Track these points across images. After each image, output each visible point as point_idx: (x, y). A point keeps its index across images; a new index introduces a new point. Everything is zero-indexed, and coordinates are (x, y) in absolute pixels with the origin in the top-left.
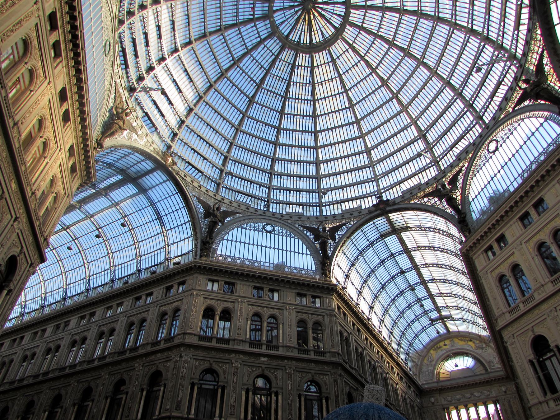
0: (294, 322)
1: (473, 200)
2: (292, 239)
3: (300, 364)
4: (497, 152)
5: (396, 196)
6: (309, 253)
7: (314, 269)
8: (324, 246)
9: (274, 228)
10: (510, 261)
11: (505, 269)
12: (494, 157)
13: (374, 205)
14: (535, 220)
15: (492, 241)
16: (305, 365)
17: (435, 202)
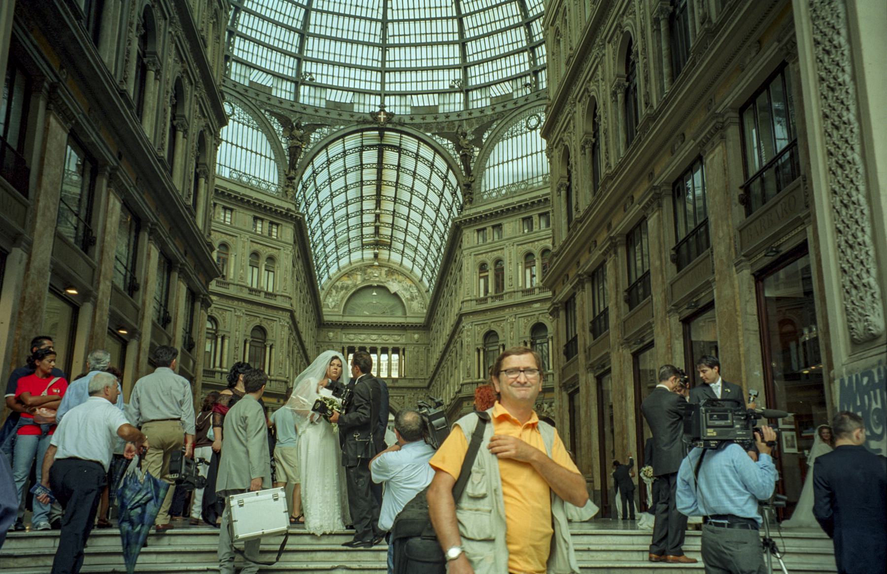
0: (247, 254)
1: (489, 167)
2: (255, 131)
3: (250, 307)
4: (534, 132)
6: (273, 157)
7: (276, 182)
8: (294, 151)
9: (233, 109)
10: (496, 254)
11: (489, 259)
12: (529, 134)
13: (372, 114)
14: (534, 230)
15: (489, 225)
16: (255, 308)
17: (448, 144)
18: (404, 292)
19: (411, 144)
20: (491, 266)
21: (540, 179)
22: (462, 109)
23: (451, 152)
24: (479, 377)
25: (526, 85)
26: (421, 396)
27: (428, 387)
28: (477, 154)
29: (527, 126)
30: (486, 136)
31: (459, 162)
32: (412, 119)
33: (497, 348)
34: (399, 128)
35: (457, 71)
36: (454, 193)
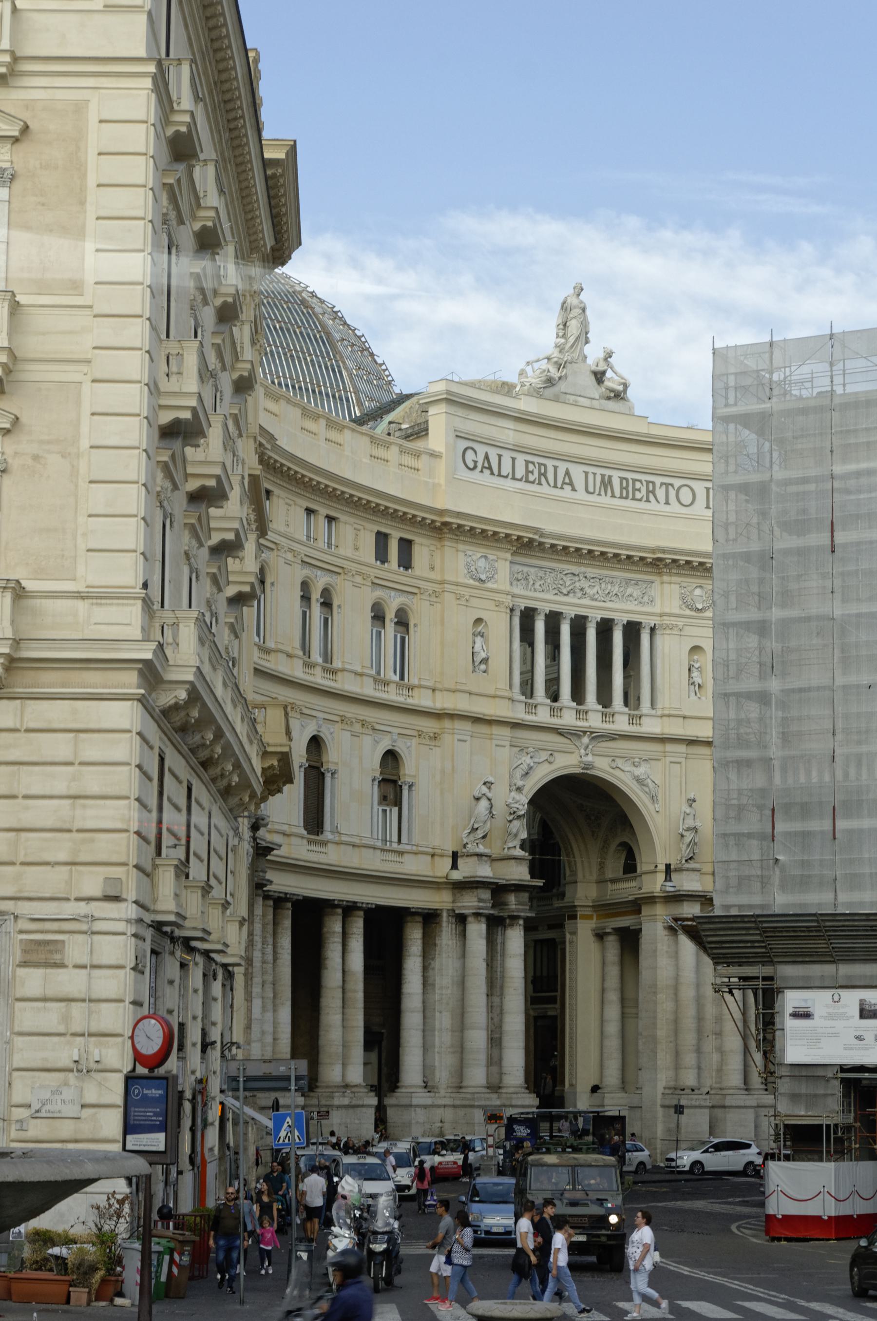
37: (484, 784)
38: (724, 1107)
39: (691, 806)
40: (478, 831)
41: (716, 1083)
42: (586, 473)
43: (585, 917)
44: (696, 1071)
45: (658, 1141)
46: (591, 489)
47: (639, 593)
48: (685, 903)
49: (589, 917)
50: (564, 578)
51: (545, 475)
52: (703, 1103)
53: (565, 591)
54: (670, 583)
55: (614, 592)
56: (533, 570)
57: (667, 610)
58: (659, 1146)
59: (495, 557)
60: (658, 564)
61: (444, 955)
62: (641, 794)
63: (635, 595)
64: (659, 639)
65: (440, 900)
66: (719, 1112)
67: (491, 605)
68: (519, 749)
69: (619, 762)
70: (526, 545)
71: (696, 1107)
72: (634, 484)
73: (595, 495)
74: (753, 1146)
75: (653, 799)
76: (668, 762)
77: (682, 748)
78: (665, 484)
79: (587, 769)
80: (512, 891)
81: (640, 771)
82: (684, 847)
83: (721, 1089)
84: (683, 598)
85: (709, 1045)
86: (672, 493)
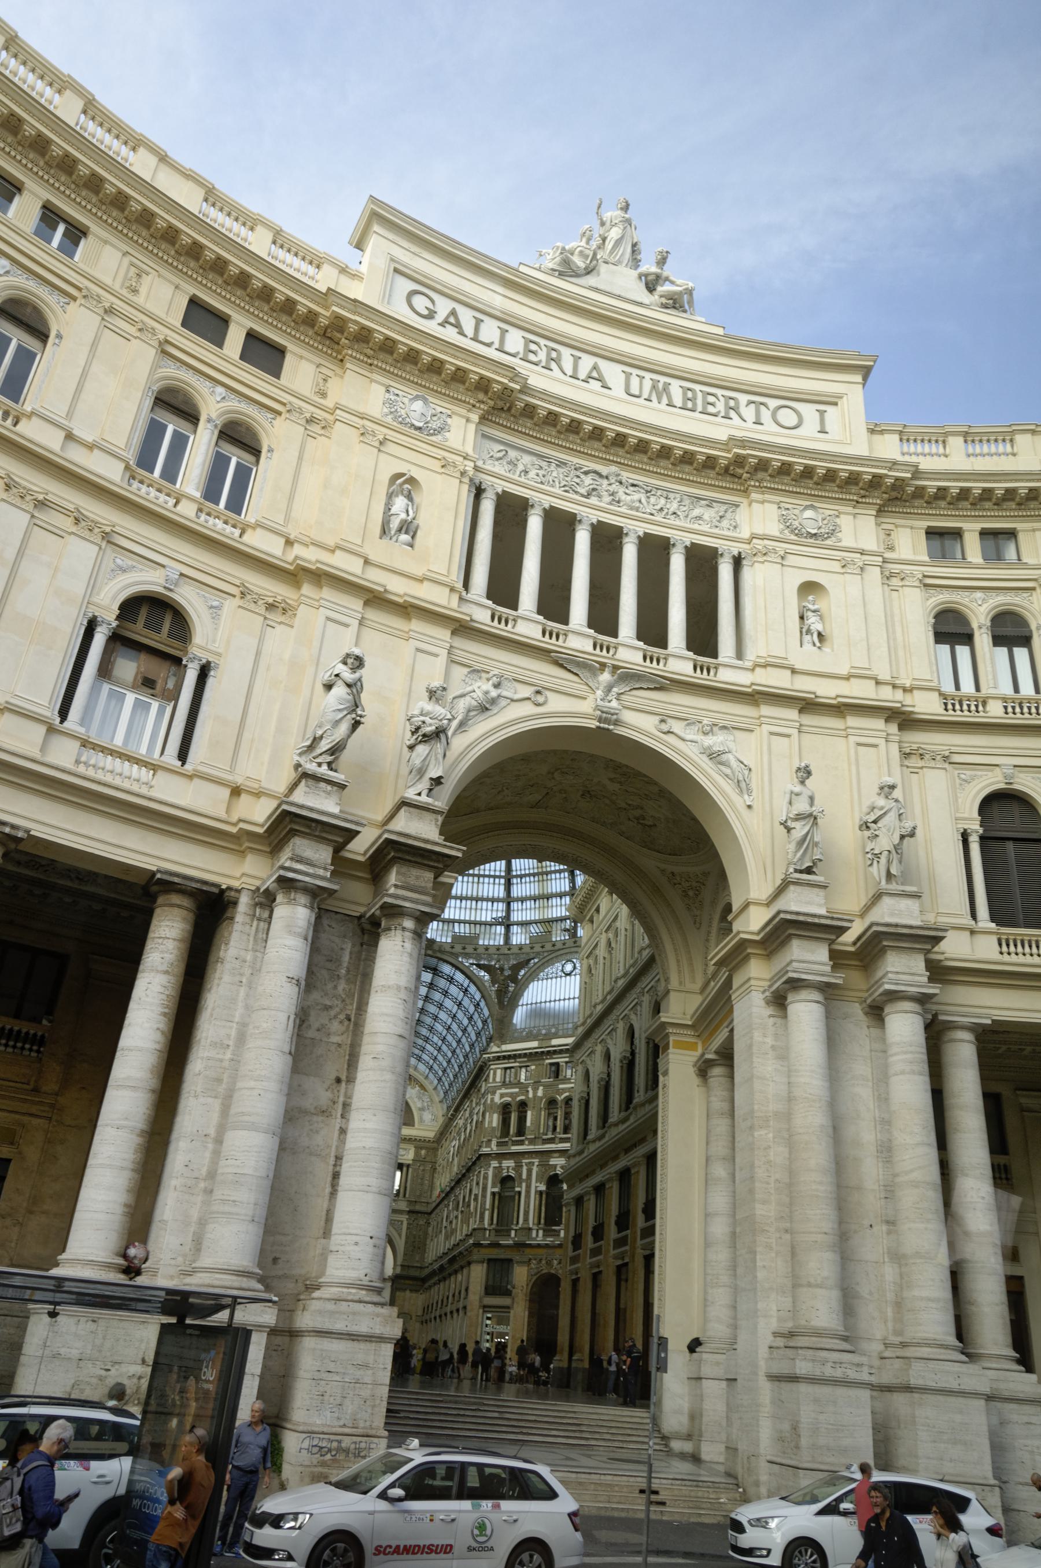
5: (444, 940)
18: (416, 1100)
19: (447, 969)
20: (514, 1108)
21: (570, 1026)
22: (502, 943)
23: (487, 984)
24: (492, 1224)
25: (566, 930)
26: (421, 1222)
27: (430, 1213)
28: (511, 989)
29: (562, 970)
30: (522, 972)
31: (494, 995)
32: (452, 947)
33: (512, 1194)
34: (439, 955)
35: (500, 904)
36: (485, 1022)
37: (345, 663)
38: (908, 1389)
39: (802, 783)
40: (323, 742)
41: (898, 1333)
42: (628, 376)
43: (680, 1045)
44: (835, 1294)
45: (763, 1465)
46: (635, 390)
47: (713, 515)
48: (795, 943)
49: (692, 1047)
50: (582, 476)
51: (557, 361)
52: (852, 1374)
53: (583, 491)
54: (763, 502)
55: (672, 510)
56: (527, 459)
57: (759, 530)
58: (764, 1478)
59: (449, 412)
60: (740, 471)
61: (227, 978)
62: (720, 780)
63: (706, 517)
64: (747, 573)
65: (241, 873)
66: (899, 1400)
67: (436, 465)
68: (469, 670)
69: (677, 727)
70: (505, 407)
71: (836, 1382)
72: (704, 398)
73: (641, 401)
74: (974, 1505)
75: (742, 786)
76: (765, 734)
77: (792, 714)
78: (753, 402)
79: (607, 721)
80: (394, 860)
81: (717, 741)
82: (792, 847)
83: (904, 1345)
84: (784, 519)
85: (871, 1246)
86: (766, 415)
